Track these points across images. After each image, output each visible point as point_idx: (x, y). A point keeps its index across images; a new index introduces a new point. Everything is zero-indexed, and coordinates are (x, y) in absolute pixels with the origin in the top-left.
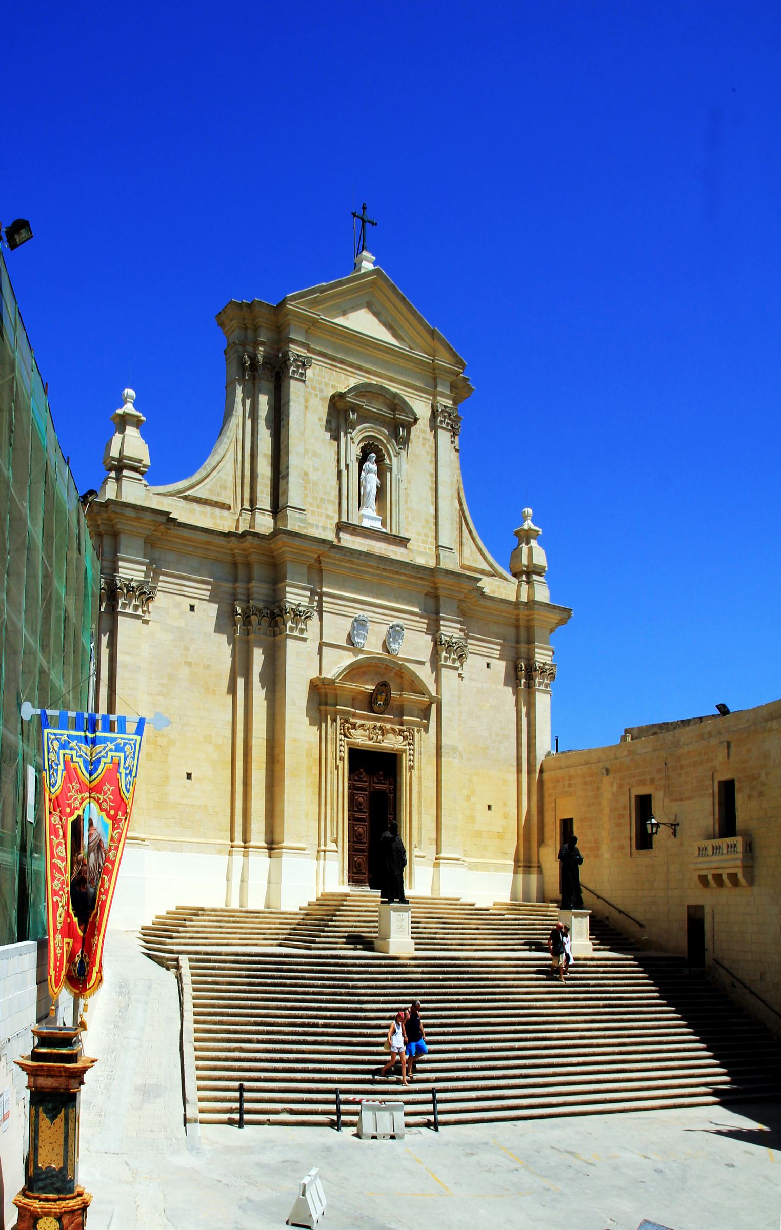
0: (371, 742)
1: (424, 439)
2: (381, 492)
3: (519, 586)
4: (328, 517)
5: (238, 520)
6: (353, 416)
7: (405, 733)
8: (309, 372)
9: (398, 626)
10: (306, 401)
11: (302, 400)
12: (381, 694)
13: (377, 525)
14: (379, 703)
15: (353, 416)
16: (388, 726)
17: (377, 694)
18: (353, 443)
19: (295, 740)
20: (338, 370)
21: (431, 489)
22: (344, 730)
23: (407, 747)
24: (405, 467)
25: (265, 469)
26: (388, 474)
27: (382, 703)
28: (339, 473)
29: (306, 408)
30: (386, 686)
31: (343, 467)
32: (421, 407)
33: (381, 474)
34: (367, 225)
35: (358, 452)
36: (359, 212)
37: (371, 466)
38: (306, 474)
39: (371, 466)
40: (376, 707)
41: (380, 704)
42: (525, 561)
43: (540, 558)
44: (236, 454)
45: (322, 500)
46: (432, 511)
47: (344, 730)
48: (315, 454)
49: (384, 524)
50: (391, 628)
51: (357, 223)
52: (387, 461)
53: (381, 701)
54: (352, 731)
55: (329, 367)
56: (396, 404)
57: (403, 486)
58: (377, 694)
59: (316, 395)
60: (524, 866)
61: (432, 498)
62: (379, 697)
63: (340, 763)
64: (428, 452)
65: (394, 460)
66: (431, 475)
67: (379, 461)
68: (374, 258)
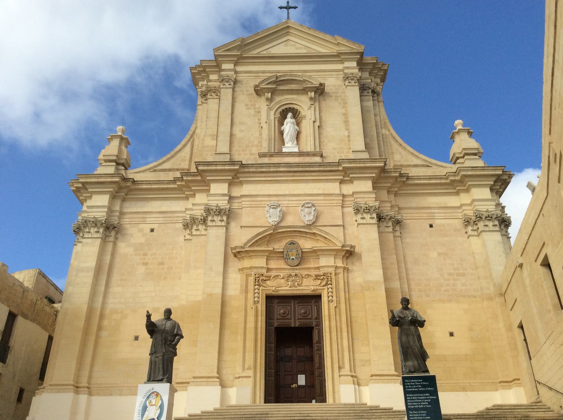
0: (287, 288)
7: (322, 277)
9: (308, 203)
12: (291, 251)
13: (296, 150)
14: (291, 258)
16: (304, 273)
17: (288, 252)
23: (326, 287)
30: (294, 244)
35: (278, 115)
37: (289, 121)
41: (293, 259)
45: (247, 146)
48: (242, 123)
50: (303, 206)
53: (292, 256)
54: (268, 282)
55: (254, 78)
58: (288, 252)
59: (243, 94)
62: (290, 253)
64: (339, 103)
66: (344, 114)
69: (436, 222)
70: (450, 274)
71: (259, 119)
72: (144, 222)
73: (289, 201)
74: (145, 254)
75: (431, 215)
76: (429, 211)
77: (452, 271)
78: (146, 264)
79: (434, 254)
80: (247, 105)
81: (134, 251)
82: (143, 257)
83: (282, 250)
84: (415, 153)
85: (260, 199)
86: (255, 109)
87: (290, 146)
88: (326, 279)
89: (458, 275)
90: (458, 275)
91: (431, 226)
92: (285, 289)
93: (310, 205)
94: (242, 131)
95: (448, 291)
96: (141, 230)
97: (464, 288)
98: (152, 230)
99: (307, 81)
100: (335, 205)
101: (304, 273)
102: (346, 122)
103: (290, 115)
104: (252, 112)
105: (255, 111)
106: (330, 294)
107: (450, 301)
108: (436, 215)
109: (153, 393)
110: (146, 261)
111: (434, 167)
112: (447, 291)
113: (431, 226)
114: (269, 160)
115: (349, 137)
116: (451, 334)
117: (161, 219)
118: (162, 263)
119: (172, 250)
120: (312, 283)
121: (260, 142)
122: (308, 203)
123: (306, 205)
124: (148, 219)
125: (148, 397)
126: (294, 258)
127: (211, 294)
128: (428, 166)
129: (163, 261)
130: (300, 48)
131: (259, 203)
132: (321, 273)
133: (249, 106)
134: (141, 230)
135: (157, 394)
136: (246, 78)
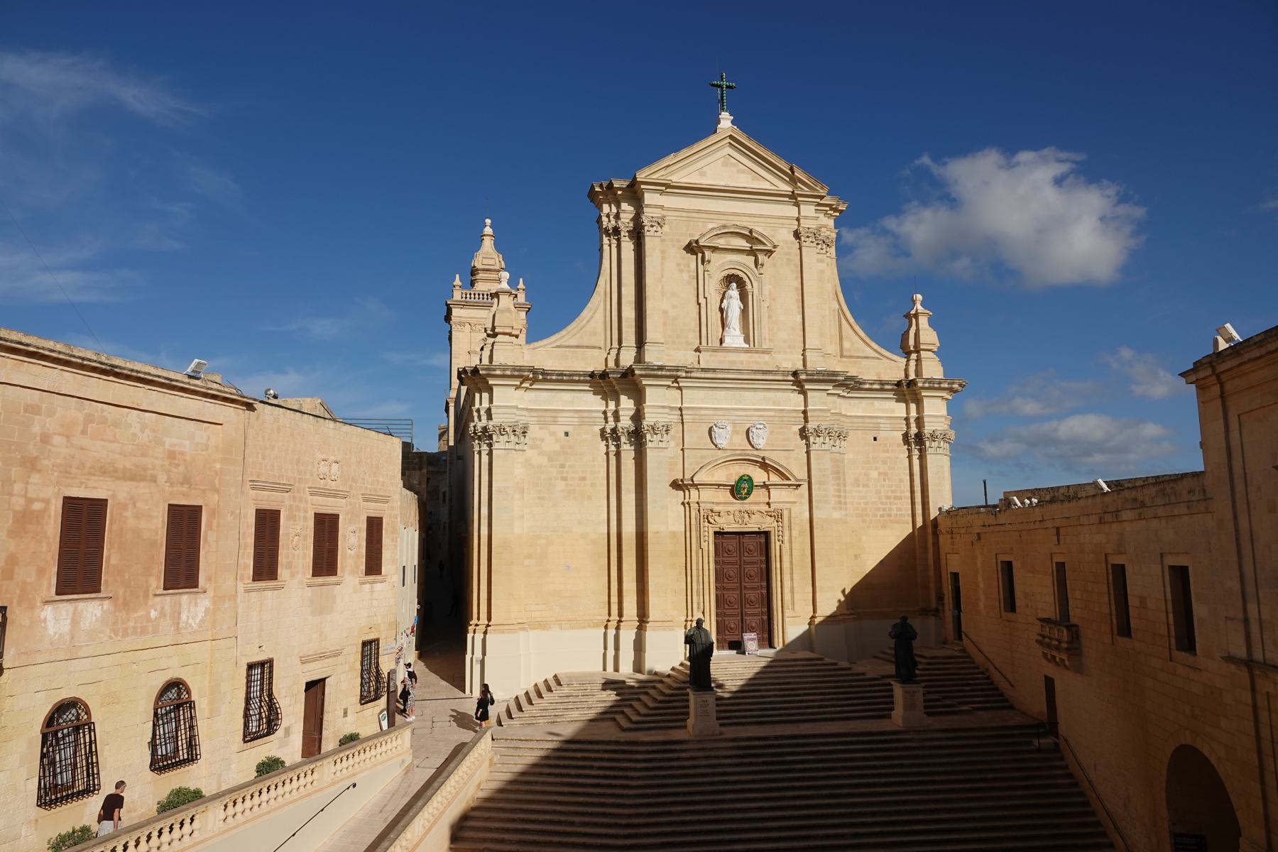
1: (788, 259)
2: (744, 312)
3: (907, 365)
4: (688, 343)
5: (606, 359)
6: (708, 254)
8: (666, 228)
15: (708, 254)
18: (711, 278)
20: (696, 220)
21: (797, 300)
22: (707, 518)
24: (767, 288)
25: (629, 313)
26: (750, 297)
28: (699, 304)
29: (663, 258)
31: (702, 301)
32: (783, 236)
33: (743, 297)
39: (734, 292)
42: (911, 342)
43: (929, 336)
44: (605, 304)
46: (799, 318)
47: (707, 518)
49: (747, 340)
52: (749, 287)
56: (750, 237)
57: (765, 304)
59: (674, 246)
61: (799, 308)
63: (704, 545)
65: (755, 284)
66: (797, 289)
67: (737, 287)
68: (732, 118)
69: (881, 435)
70: (888, 498)
72: (555, 423)
73: (736, 416)
74: (563, 466)
75: (877, 425)
76: (875, 421)
77: (890, 494)
78: (564, 479)
79: (874, 474)
80: (679, 265)
81: (549, 461)
82: (561, 469)
83: (733, 483)
84: (868, 340)
85: (703, 412)
86: (689, 272)
89: (896, 498)
90: (896, 498)
91: (875, 439)
92: (734, 527)
93: (762, 426)
94: (674, 307)
95: (884, 517)
96: (553, 434)
97: (899, 513)
98: (567, 434)
99: (757, 238)
100: (786, 423)
101: (755, 508)
104: (686, 276)
105: (690, 276)
106: (780, 533)
107: (884, 527)
108: (881, 425)
110: (565, 475)
111: (885, 360)
112: (881, 516)
113: (875, 439)
114: (711, 355)
117: (576, 420)
118: (584, 479)
119: (593, 461)
120: (761, 520)
122: (760, 424)
123: (758, 426)
124: (560, 419)
127: (658, 532)
128: (879, 359)
129: (584, 475)
130: (743, 172)
131: (704, 417)
132: (772, 509)
133: (682, 267)
134: (553, 434)
136: (675, 218)
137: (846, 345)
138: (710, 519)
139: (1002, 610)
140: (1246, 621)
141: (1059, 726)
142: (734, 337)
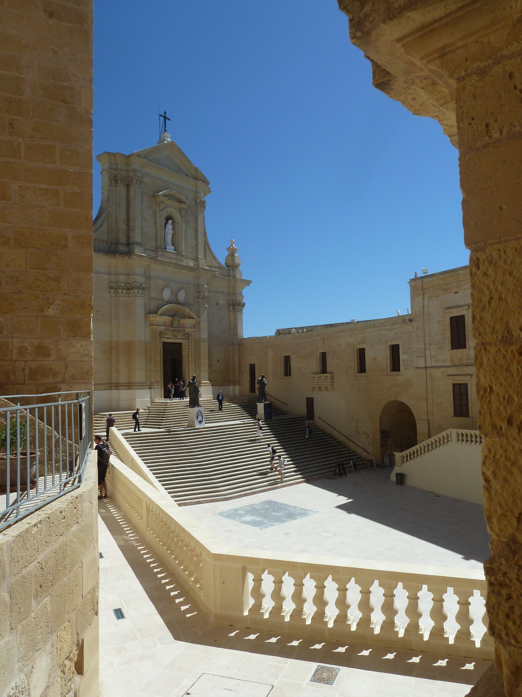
10: (142, 197)
11: (140, 198)
19: (140, 341)
27: (176, 323)
29: (142, 200)
31: (158, 226)
34: (167, 120)
36: (163, 115)
38: (142, 229)
40: (174, 325)
46: (195, 242)
51: (162, 119)
54: (165, 336)
60: (233, 383)
71: (155, 220)
80: (148, 206)
87: (170, 248)
88: (187, 336)
91: (217, 304)
102: (196, 234)
103: (170, 222)
109: (199, 411)
113: (217, 304)
115: (197, 245)
116: (218, 361)
121: (157, 238)
125: (198, 413)
126: (176, 323)
135: (201, 412)
137: (208, 258)
138: (162, 335)
139: (283, 376)
140: (425, 356)
141: (315, 415)
142: (170, 248)
